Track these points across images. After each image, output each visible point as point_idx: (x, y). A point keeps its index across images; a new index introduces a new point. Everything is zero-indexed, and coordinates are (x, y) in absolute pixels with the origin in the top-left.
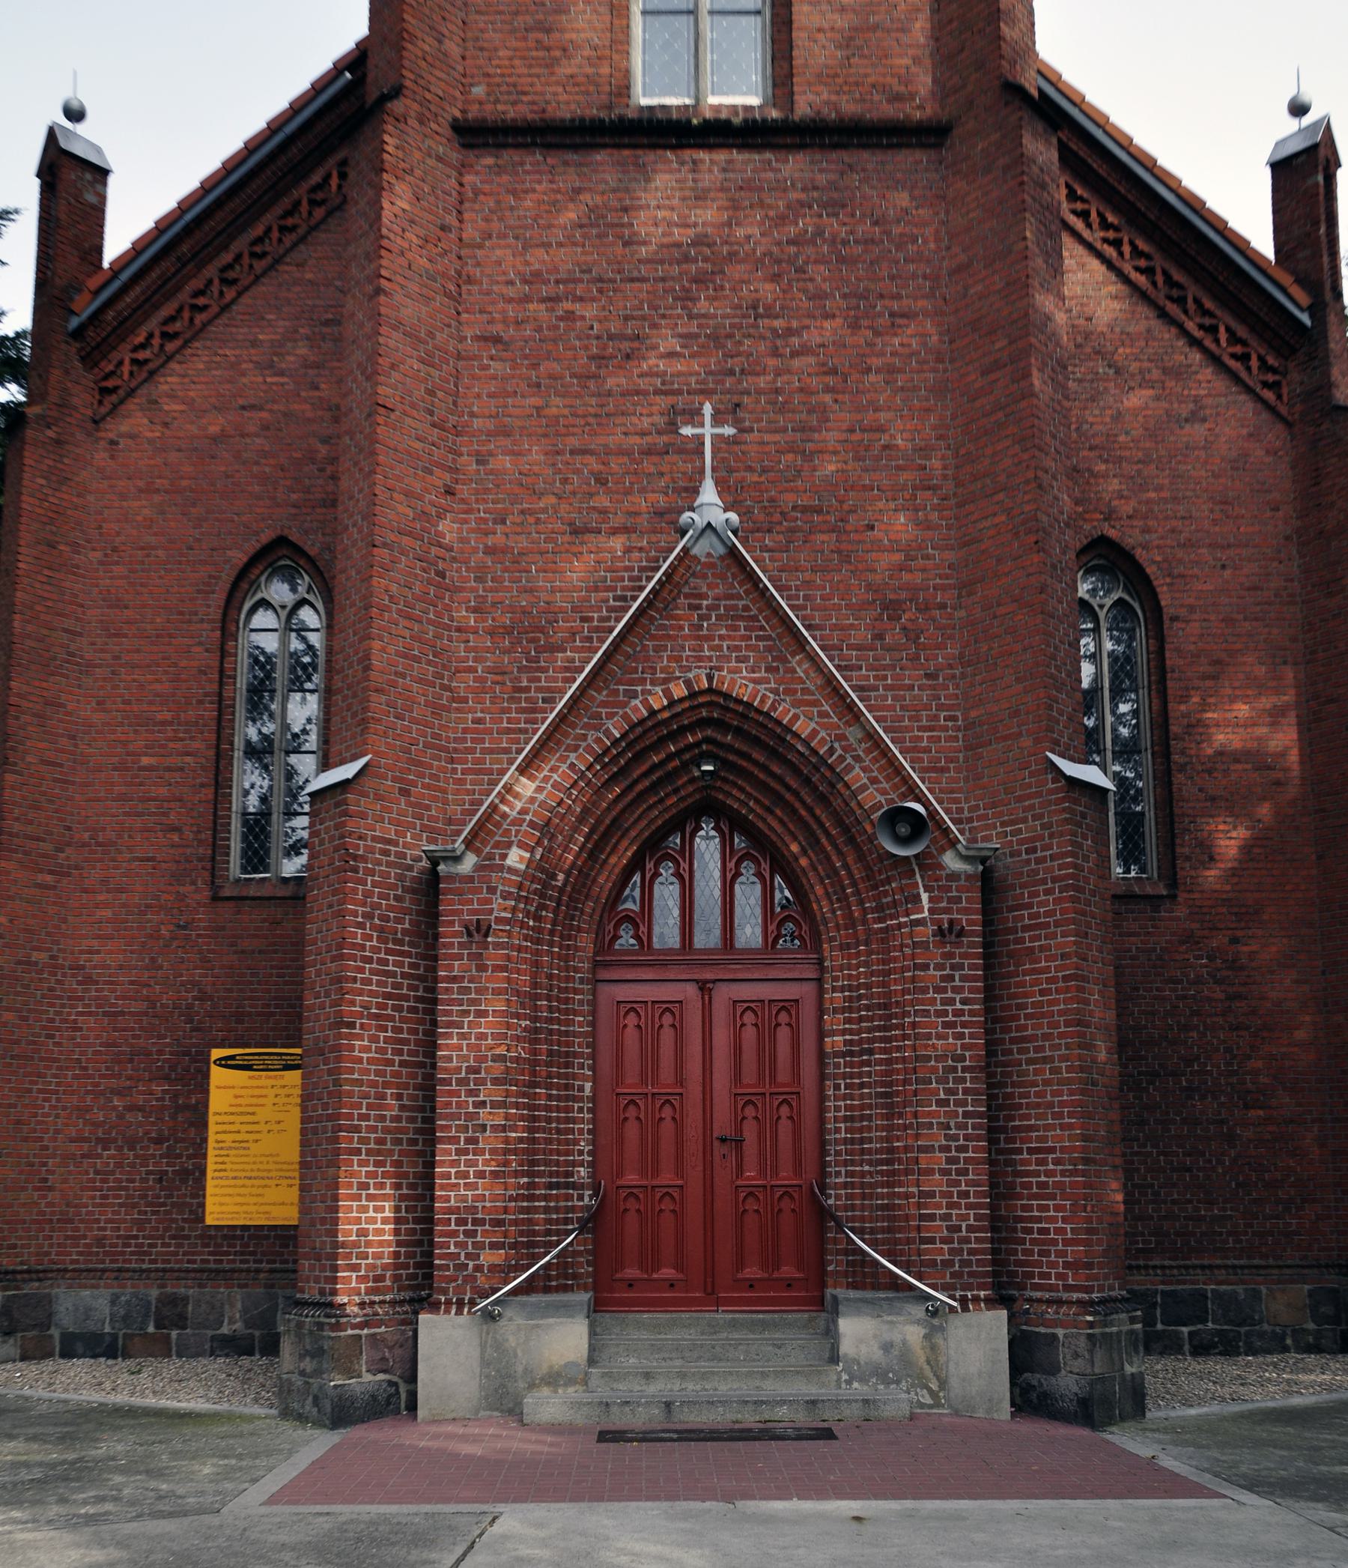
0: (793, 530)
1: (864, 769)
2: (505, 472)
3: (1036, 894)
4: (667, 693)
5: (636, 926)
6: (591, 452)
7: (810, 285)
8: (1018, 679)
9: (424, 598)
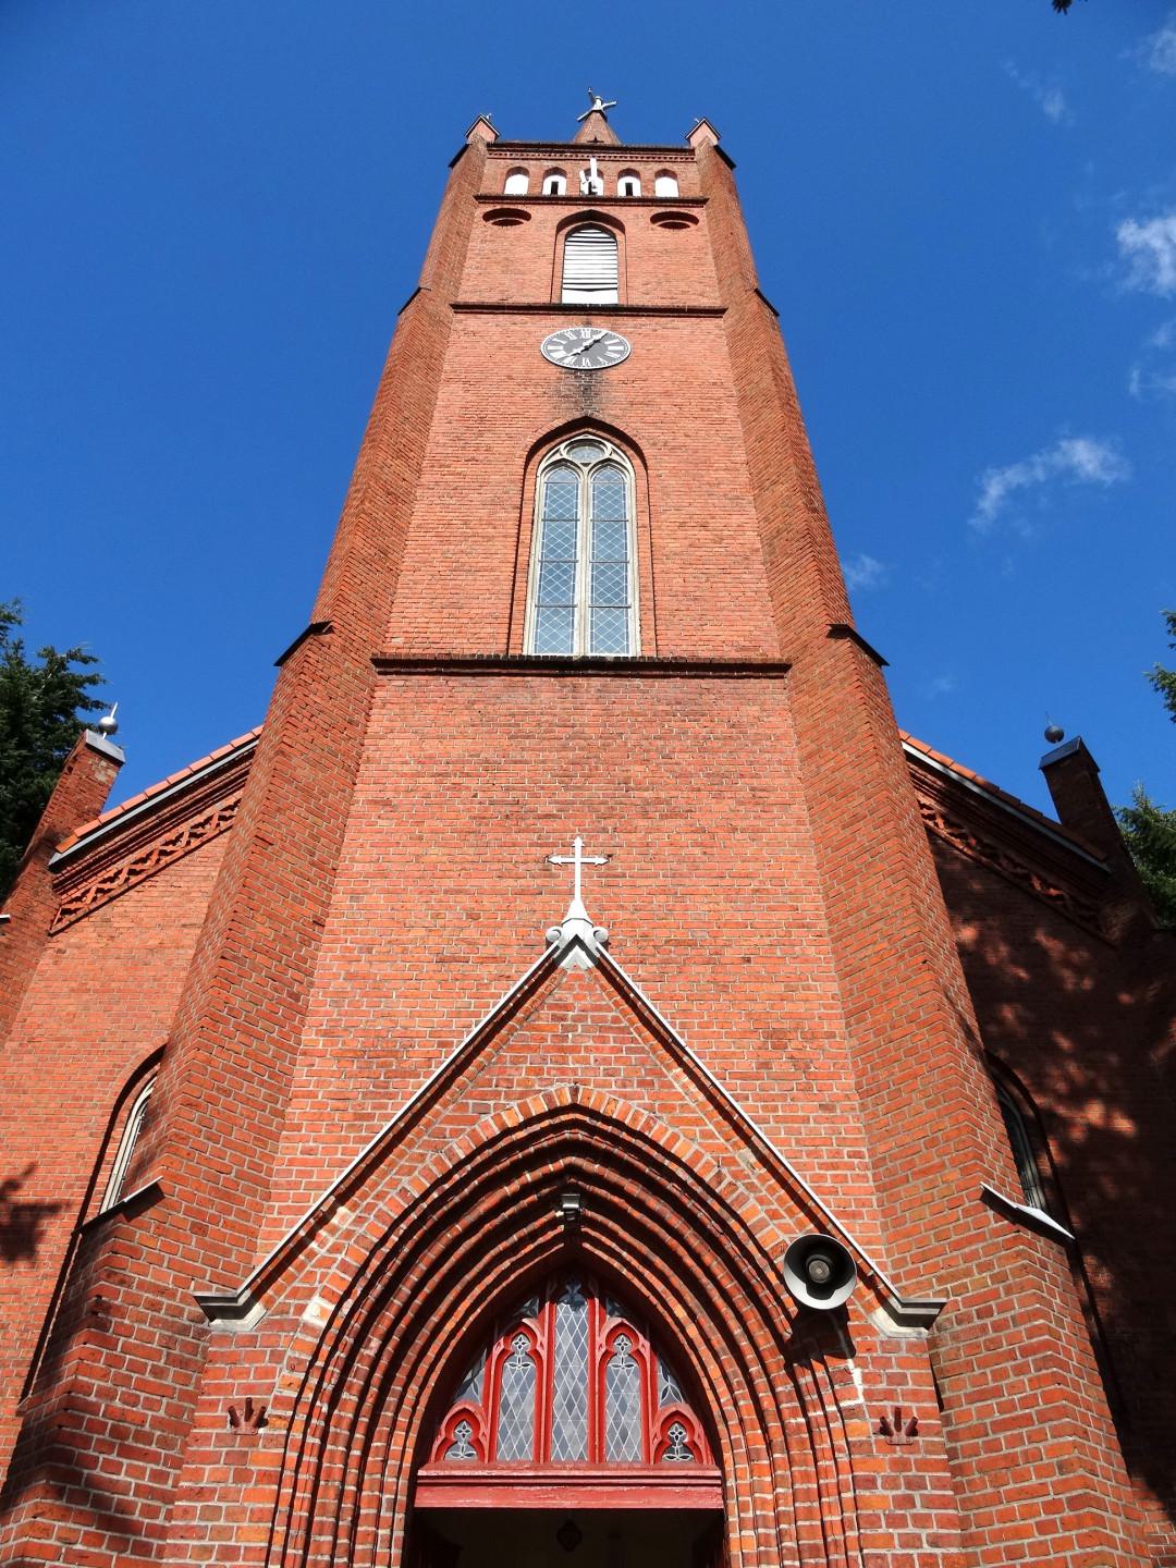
0: (666, 962)
1: (761, 1201)
2: (378, 907)
3: (1003, 1374)
4: (523, 1108)
5: (475, 1424)
6: (466, 892)
7: (676, 768)
8: (929, 1104)
9: (270, 1016)
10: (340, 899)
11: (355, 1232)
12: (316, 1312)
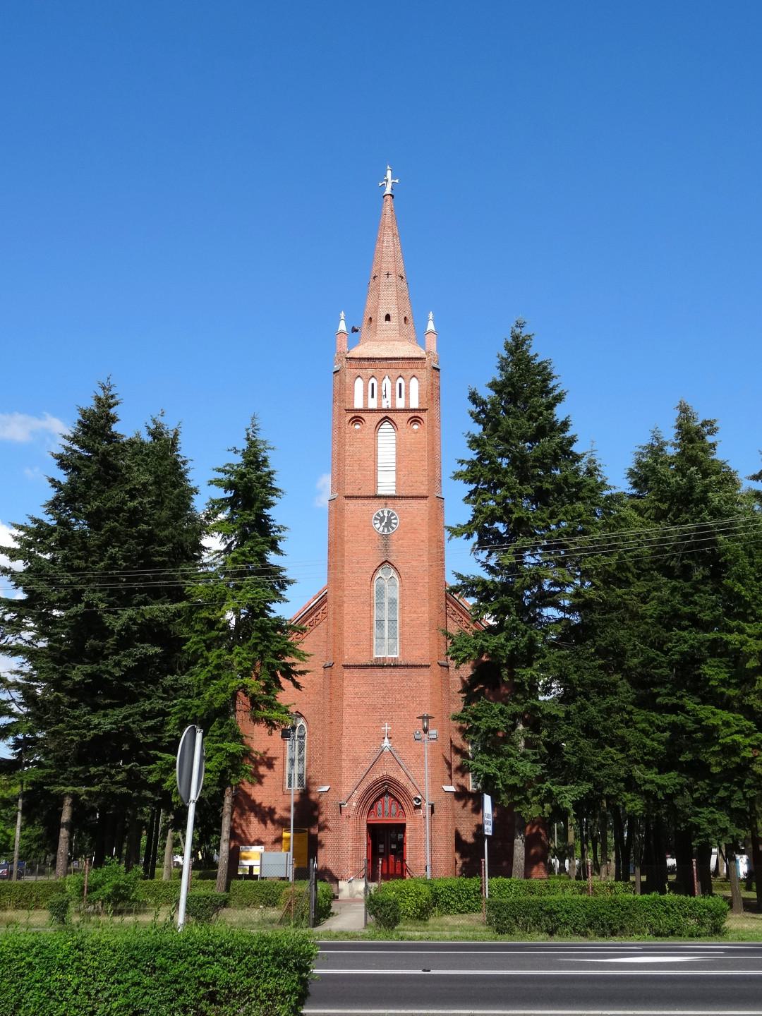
12: (354, 804)
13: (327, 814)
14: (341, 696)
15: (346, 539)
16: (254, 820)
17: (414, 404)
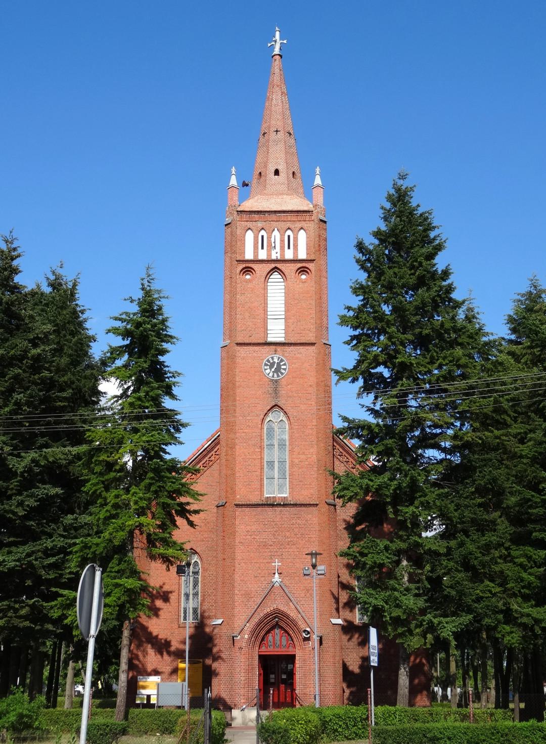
10: (237, 565)
11: (249, 627)
12: (246, 636)
13: (221, 645)
14: (234, 533)
15: (237, 384)
16: (151, 651)
17: (302, 255)
